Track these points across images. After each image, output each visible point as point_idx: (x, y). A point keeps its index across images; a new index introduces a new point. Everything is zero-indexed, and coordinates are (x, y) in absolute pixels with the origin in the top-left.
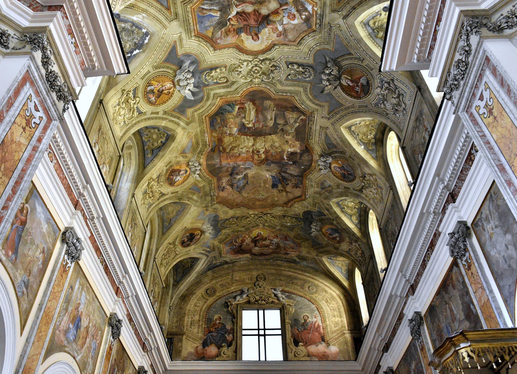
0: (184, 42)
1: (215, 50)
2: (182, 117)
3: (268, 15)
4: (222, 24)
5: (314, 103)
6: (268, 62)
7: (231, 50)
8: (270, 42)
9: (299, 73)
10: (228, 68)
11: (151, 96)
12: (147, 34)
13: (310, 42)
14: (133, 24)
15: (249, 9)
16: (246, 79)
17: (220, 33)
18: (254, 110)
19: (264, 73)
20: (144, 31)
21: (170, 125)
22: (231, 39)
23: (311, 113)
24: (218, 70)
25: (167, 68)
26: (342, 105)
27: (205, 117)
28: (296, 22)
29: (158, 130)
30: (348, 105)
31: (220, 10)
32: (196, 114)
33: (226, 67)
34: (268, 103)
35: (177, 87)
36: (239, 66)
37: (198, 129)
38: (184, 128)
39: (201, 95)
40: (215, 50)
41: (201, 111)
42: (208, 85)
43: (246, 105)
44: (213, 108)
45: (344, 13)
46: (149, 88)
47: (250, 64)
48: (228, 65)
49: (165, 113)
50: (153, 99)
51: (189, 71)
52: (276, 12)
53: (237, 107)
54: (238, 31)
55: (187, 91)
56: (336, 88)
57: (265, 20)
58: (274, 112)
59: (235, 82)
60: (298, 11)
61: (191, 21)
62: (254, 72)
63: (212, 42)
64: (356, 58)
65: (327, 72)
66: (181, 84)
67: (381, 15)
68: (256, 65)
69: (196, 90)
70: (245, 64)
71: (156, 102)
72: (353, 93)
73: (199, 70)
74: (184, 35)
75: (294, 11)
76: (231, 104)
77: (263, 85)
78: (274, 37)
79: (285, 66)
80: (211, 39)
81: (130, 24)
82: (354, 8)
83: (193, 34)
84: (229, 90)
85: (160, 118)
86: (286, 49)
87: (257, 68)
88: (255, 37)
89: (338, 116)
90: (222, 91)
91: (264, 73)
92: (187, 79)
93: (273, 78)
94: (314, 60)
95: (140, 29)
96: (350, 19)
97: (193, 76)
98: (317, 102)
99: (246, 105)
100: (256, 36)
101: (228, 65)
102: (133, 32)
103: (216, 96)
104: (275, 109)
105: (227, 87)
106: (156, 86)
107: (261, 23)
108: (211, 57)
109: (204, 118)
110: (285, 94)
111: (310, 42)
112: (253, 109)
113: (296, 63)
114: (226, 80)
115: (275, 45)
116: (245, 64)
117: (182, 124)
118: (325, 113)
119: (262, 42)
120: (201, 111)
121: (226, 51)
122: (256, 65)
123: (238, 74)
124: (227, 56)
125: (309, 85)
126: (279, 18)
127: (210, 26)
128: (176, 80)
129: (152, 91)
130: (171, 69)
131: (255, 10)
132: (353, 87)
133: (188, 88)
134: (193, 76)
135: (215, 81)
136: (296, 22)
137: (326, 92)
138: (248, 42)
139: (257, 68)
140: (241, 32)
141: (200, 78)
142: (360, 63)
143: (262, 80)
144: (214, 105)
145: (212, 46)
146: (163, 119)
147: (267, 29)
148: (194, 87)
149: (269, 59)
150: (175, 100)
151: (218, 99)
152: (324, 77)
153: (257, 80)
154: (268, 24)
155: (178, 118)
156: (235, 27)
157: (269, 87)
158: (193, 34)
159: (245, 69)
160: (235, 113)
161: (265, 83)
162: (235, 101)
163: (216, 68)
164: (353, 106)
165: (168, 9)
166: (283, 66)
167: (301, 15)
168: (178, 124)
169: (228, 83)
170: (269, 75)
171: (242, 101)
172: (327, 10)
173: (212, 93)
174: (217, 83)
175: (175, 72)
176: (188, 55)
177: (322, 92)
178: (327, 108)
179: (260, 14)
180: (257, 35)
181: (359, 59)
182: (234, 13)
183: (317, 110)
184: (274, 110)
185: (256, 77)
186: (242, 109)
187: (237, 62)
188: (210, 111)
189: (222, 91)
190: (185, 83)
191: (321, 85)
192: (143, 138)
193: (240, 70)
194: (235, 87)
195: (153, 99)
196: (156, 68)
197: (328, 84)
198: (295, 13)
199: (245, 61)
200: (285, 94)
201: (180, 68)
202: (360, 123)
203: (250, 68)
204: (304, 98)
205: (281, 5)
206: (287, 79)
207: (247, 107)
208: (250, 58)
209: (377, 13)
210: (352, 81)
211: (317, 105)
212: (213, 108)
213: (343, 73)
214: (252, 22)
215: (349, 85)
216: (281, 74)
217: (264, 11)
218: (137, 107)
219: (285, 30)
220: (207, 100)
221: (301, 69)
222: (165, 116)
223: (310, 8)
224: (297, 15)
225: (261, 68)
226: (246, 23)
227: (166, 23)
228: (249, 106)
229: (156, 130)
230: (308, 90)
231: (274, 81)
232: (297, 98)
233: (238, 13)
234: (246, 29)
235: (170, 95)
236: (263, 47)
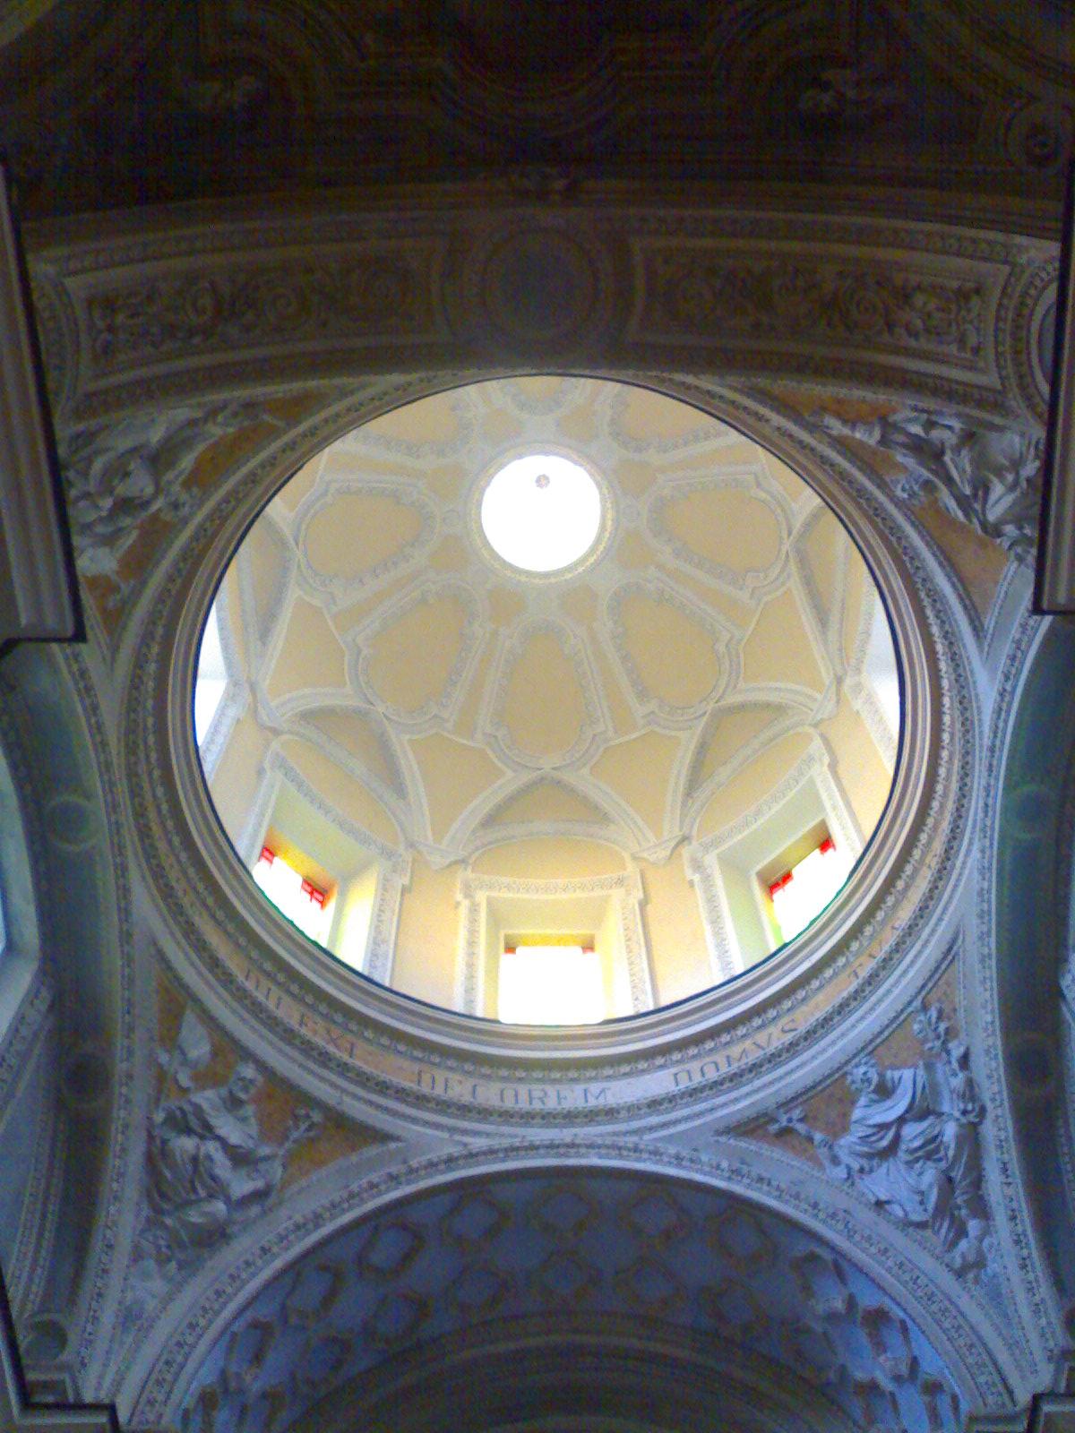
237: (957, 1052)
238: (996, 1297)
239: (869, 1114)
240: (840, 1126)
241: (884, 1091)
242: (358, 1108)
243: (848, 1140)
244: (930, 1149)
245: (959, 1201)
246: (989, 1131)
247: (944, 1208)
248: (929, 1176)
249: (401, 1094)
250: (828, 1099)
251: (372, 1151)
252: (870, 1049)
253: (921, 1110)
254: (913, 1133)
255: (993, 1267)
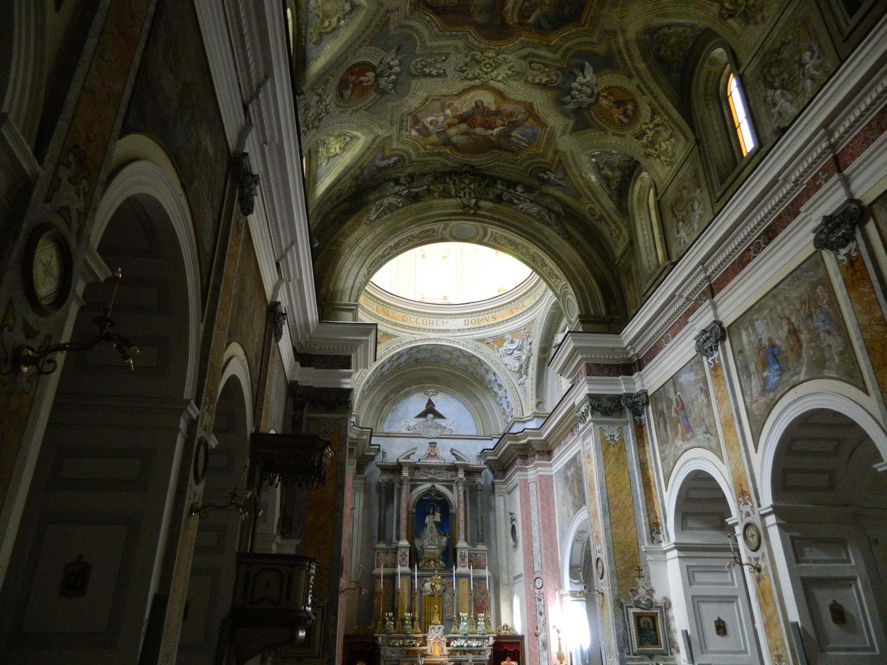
0: (561, 128)
1: (531, 104)
2: (615, 49)
3: (459, 123)
4: (514, 125)
5: (411, 27)
6: (470, 76)
7: (513, 97)
8: (462, 98)
9: (430, 65)
10: (524, 78)
11: (629, 112)
12: (593, 156)
13: (413, 103)
14: (598, 169)
15: (479, 130)
16: (505, 59)
17: (519, 118)
18: (506, 9)
19: (478, 62)
20: (594, 160)
21: (636, 53)
22: (508, 107)
23: (415, 10)
24: (537, 81)
25: (593, 119)
26: (370, 44)
27: (584, 26)
28: (429, 119)
29: (659, 50)
30: (362, 50)
31: (510, 136)
32: (594, 39)
33: (526, 81)
34: (481, 19)
35: (596, 92)
36: (508, 77)
37: (605, 12)
38: (624, 31)
39: (574, 61)
40: (531, 104)
41: (585, 39)
42: (558, 68)
43: (516, 20)
44: (567, 33)
45: (378, 140)
46: (626, 121)
47: (494, 76)
48: (522, 81)
49: (630, 77)
50: (630, 106)
51: (573, 98)
52: (450, 125)
53: (531, 20)
54: (498, 113)
55: (588, 77)
56: (381, 63)
57: (462, 119)
58: (474, 3)
59: (521, 58)
60: (427, 128)
61: (544, 141)
62: (491, 65)
63: (530, 111)
64: (361, 108)
65: (393, 77)
66: (589, 91)
67: (340, 148)
68: (486, 73)
69: (576, 72)
70: (500, 78)
71: (631, 100)
72: (356, 69)
73: (560, 93)
74: (558, 133)
75: (431, 128)
76: (538, 28)
77: (482, 46)
78: (457, 103)
79: (448, 72)
80: (530, 116)
81: (602, 172)
82: (368, 149)
83: (548, 129)
84: (533, 51)
85: (641, 78)
86: (444, 91)
87: (485, 70)
88: (480, 104)
89: (374, 24)
90: (543, 53)
91: (478, 62)
92: (580, 91)
93: (467, 56)
94: (410, 83)
95: (596, 163)
96: (371, 137)
97: (572, 89)
98: (407, 31)
99: (516, 20)
100: (478, 105)
101: (522, 81)
102: (605, 163)
103: (554, 49)
104: (472, 8)
105: (533, 55)
106: (617, 114)
107: (470, 116)
108: (540, 100)
109: (587, 25)
110: (454, 33)
111: (413, 103)
112: (507, 12)
113: (433, 76)
114: (533, 65)
115: (457, 95)
116: (500, 78)
117: (621, 41)
118: (394, 17)
119: (473, 98)
120: (585, 39)
121: (519, 98)
122: (486, 73)
123: (513, 67)
124: (519, 91)
125: (417, 51)
126: (448, 120)
127: (527, 127)
128: (592, 100)
129: (625, 114)
130: (590, 114)
131: (474, 128)
132: (359, 75)
133: (584, 81)
134: (572, 89)
135: (547, 69)
136: (429, 119)
137: (394, 50)
138: (488, 100)
139: (485, 70)
140: (495, 112)
141: (564, 83)
142: (354, 108)
143: (482, 53)
144: (563, 37)
145: (533, 109)
146: (638, 72)
147: (464, 110)
148: (576, 77)
149: (467, 79)
150: (610, 79)
151: (553, 43)
152: (397, 69)
153: (490, 54)
154: (461, 115)
155: (620, 53)
156: (499, 117)
157: (476, 43)
158: (548, 129)
159: (502, 72)
160: (537, 12)
161: (479, 49)
162: (530, 31)
163: (539, 84)
164: (354, 53)
165: (560, 162)
166: (450, 72)
167: (424, 125)
168: (626, 44)
169: (530, 59)
170: (471, 60)
171: (520, 28)
172: (395, 136)
173: (558, 56)
174: (545, 65)
175: (588, 108)
176: (565, 114)
177: (398, 49)
178: (392, 27)
179: (469, 124)
180: (477, 106)
181: (356, 111)
182: (496, 130)
183: (406, 18)
184: (475, 6)
185: (489, 58)
186: (524, 14)
187: (510, 81)
188: (573, 30)
189: (543, 53)
190: (584, 88)
191: (399, 57)
192: (691, 44)
193: (509, 72)
194: (524, 52)
195: (630, 106)
196: (604, 130)
197: (392, 63)
198: (429, 126)
199: (499, 81)
200: (454, 33)
201: (580, 108)
202: (339, 20)
203: (495, 72)
204: (425, 33)
205: (444, 131)
206: (447, 55)
207: (515, 17)
208: (492, 83)
209: (344, 150)
210: (362, 82)
211: (405, 27)
212: (567, 33)
213: (373, 85)
214: (479, 118)
215: (364, 76)
216: (455, 60)
217: (464, 127)
218: (651, 122)
219: (443, 110)
220: (568, 50)
221: (427, 70)
222: (634, 73)
223: (414, 133)
224: (428, 125)
225: (481, 70)
226: (487, 119)
227: (569, 154)
228: (511, 17)
229: (662, 52)
230: (418, 44)
231: (466, 52)
232: (437, 30)
233: (493, 129)
234: (486, 113)
235: (610, 90)
236: (472, 94)
237: (530, 341)
238: (525, 391)
239: (507, 345)
240: (501, 345)
241: (512, 342)
242: (390, 331)
243: (501, 349)
244: (519, 358)
245: (522, 371)
246: (532, 358)
247: (519, 371)
248: (517, 364)
249: (400, 326)
250: (499, 340)
251: (394, 339)
252: (511, 332)
253: (520, 349)
254: (515, 352)
255: (526, 385)
